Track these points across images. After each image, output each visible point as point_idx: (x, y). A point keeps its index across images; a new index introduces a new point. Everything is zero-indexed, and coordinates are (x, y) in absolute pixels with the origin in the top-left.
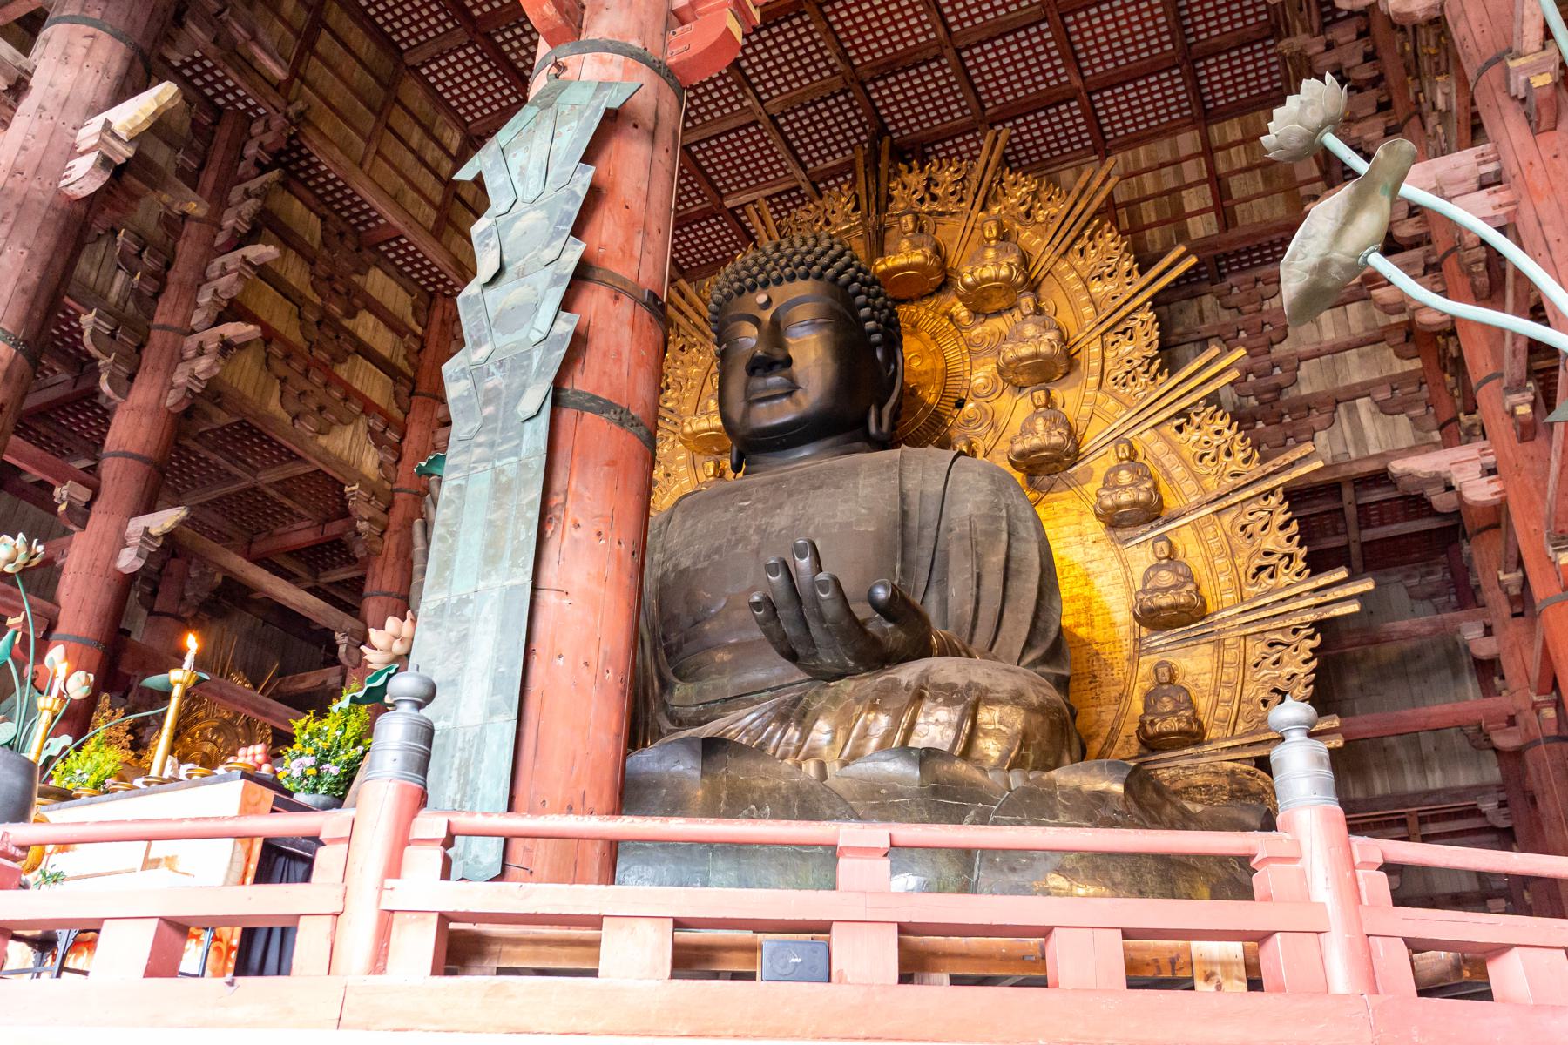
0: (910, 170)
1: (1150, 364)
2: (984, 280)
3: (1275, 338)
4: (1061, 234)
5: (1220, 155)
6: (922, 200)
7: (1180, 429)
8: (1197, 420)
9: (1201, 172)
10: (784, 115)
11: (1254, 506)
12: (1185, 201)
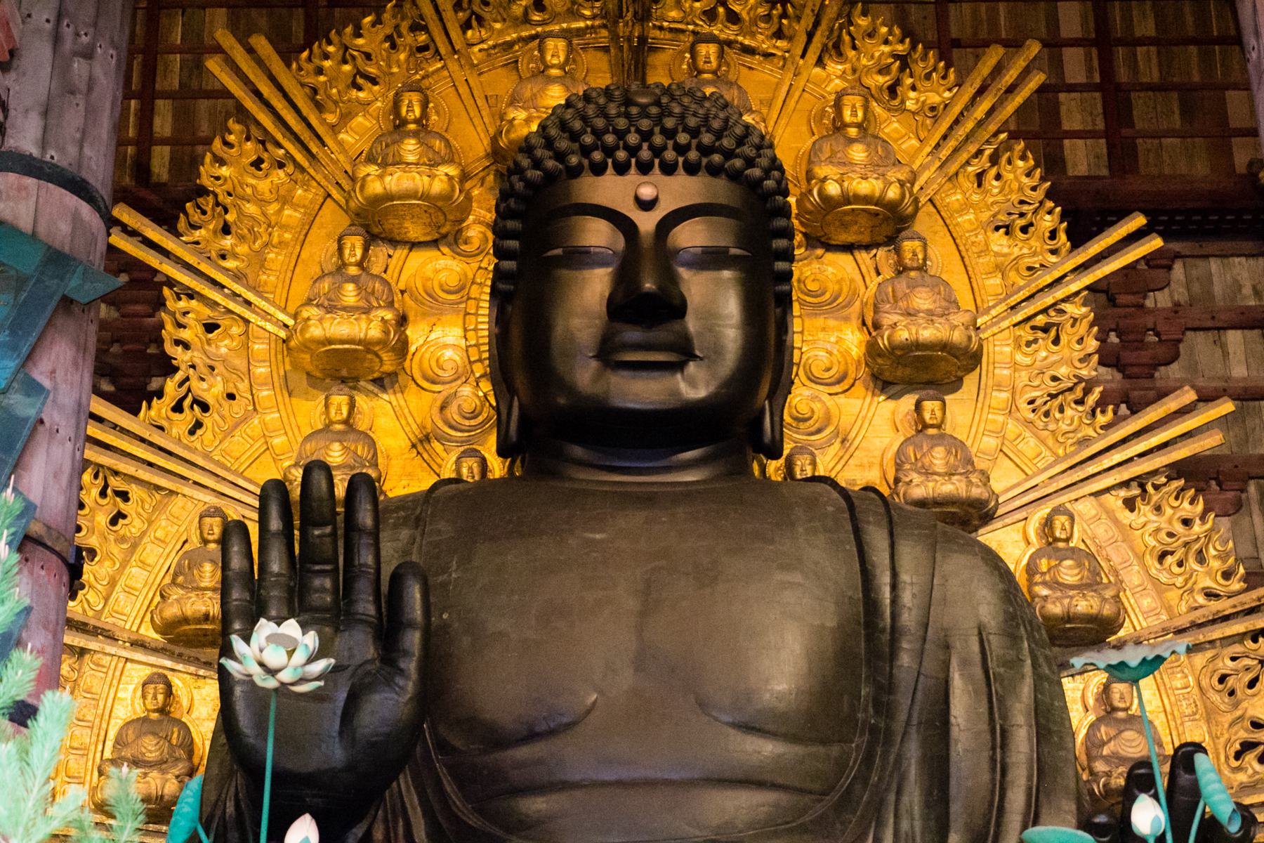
1: (1087, 391)
2: (858, 199)
3: (1161, 351)
4: (952, 143)
5: (1121, 51)
6: (710, 15)
7: (1130, 504)
8: (1156, 497)
9: (1090, 70)
11: (1237, 649)
12: (1063, 109)
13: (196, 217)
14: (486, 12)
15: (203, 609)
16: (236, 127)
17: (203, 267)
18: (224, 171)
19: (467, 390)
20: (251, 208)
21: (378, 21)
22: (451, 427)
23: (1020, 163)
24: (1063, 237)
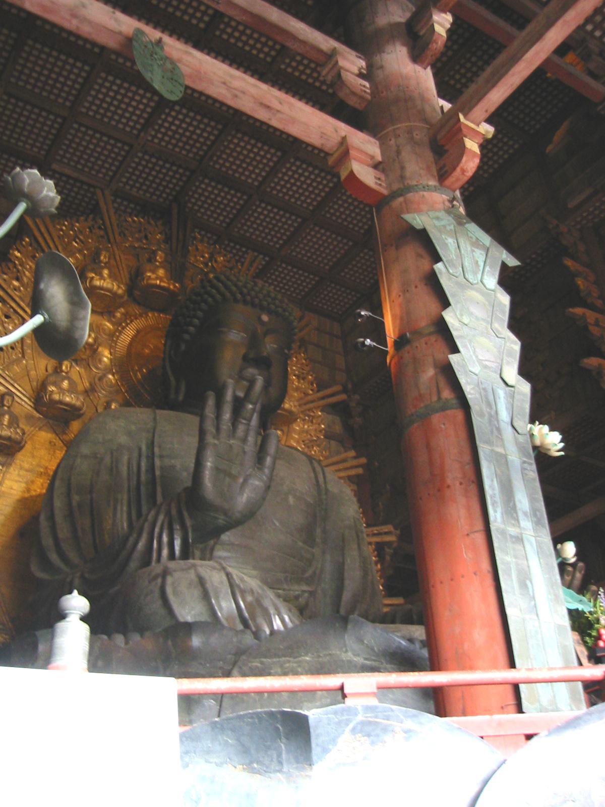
0: (202, 241)
10: (145, 153)
13: (6, 270)
14: (126, 232)
15: (9, 434)
16: (27, 240)
17: (9, 291)
18: (19, 255)
19: (110, 376)
20: (27, 273)
21: (86, 220)
22: (102, 388)
23: (303, 355)
24: (315, 385)
